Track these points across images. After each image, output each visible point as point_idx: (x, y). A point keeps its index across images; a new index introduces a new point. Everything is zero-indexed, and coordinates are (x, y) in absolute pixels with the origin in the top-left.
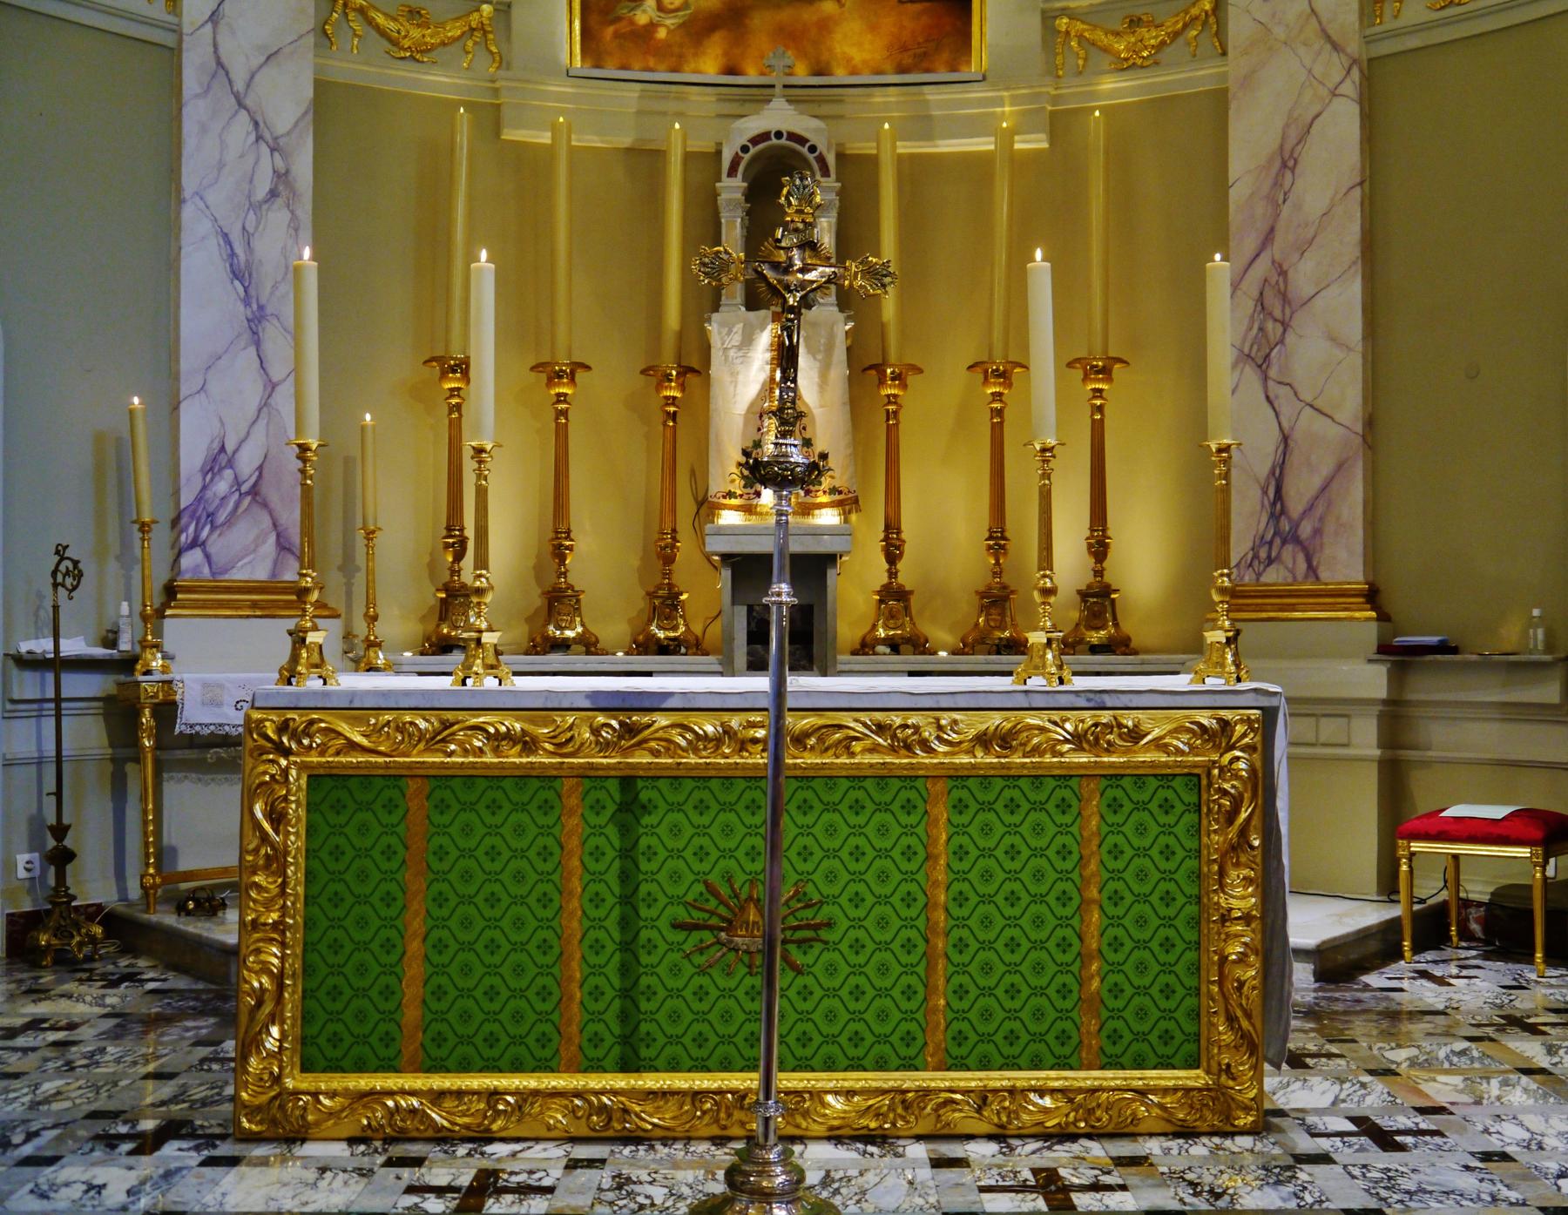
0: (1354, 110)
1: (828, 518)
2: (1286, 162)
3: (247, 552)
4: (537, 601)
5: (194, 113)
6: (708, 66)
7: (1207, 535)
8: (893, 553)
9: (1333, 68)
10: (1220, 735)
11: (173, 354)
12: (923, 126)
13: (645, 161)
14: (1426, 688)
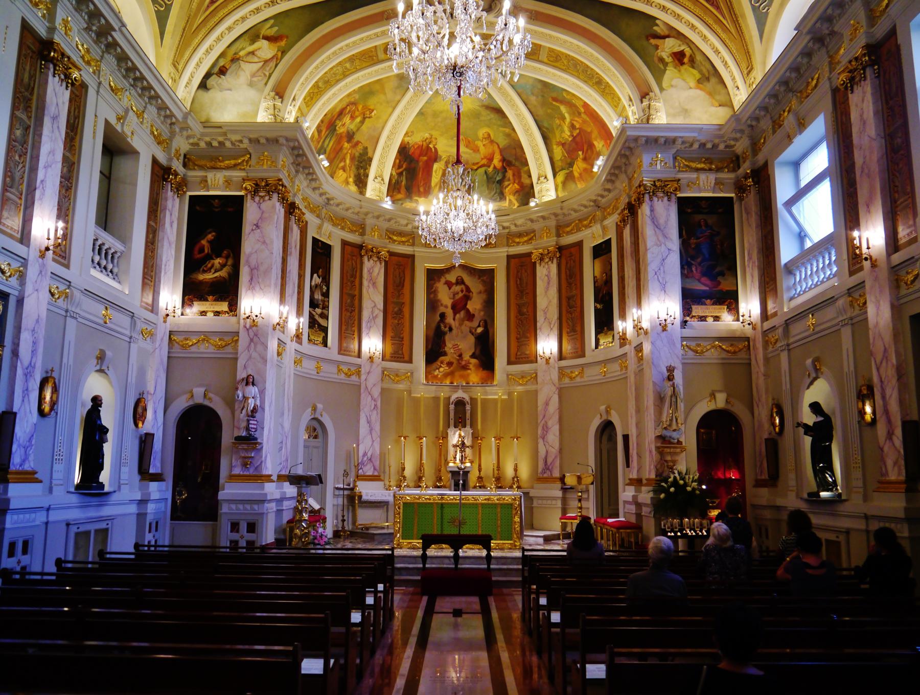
1: (468, 465)
2: (547, 404)
3: (369, 470)
4: (416, 478)
5: (363, 395)
6: (448, 382)
9: (554, 389)
10: (515, 499)
11: (358, 436)
12: (486, 393)
13: (436, 399)
14: (569, 495)
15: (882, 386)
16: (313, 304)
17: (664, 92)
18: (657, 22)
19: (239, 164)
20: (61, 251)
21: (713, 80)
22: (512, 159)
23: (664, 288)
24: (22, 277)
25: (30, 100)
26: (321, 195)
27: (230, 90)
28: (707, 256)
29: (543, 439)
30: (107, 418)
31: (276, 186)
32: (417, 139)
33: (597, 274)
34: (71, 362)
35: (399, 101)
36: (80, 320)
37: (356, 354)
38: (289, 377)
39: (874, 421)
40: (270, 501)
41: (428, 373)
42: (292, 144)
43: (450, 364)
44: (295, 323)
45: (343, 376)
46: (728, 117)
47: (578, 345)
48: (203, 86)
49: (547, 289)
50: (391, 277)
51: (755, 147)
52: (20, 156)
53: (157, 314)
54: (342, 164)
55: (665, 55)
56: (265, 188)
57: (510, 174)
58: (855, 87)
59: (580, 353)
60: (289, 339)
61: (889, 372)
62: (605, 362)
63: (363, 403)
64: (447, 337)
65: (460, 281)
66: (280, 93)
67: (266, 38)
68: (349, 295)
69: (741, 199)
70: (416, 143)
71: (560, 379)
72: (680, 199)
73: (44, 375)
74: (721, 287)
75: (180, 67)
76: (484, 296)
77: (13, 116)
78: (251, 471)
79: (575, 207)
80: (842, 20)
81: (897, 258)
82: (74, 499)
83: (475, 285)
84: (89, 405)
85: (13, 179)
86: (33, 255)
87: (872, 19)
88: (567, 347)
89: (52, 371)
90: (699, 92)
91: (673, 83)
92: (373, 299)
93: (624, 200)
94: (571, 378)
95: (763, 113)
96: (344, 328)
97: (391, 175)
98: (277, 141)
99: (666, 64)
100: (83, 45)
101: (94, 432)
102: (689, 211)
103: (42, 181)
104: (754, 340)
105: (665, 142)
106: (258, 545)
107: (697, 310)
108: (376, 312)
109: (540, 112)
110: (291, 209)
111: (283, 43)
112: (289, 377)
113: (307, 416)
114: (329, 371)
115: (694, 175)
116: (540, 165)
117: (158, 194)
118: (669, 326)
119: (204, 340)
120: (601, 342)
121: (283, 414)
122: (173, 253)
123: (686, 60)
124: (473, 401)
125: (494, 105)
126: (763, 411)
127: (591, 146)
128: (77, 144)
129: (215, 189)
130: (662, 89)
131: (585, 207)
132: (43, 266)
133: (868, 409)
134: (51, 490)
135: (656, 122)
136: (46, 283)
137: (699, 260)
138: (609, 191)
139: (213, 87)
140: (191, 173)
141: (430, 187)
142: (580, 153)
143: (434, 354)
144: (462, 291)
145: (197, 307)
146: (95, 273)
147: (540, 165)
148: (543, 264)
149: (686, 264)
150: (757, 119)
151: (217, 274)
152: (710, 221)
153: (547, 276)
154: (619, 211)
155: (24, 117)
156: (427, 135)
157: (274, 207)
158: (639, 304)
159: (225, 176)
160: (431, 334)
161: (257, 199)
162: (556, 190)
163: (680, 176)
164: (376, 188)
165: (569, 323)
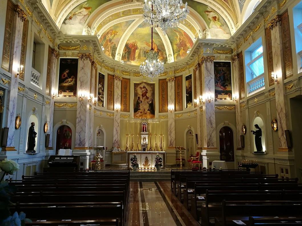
2: (171, 125)
6: (141, 118)
7: (167, 144)
8: (151, 145)
15: (280, 120)
16: (99, 94)
17: (210, 29)
18: (208, 7)
19: (77, 48)
20: (22, 75)
21: (225, 26)
22: (160, 49)
23: (210, 90)
24: (9, 83)
25: (11, 24)
26: (101, 59)
27: (73, 24)
28: (222, 79)
29: (170, 135)
30: (36, 130)
31: (89, 55)
32: (131, 42)
33: (187, 85)
34: (25, 111)
35: (126, 30)
36: (27, 98)
37: (113, 109)
38: (93, 116)
39: (277, 130)
40: (88, 155)
41: (134, 115)
42: (94, 43)
43: (141, 112)
44: (95, 99)
45: (108, 116)
46: (230, 38)
47: (181, 107)
48: (64, 23)
50: (123, 86)
51: (238, 47)
52: (8, 43)
53: (51, 96)
54: (108, 49)
55: (210, 18)
56: (85, 56)
57: (160, 54)
58: (273, 28)
59: (181, 109)
60: (92, 104)
61: (283, 116)
62: (190, 112)
63: (115, 124)
64: (140, 104)
65: (144, 87)
66: (89, 26)
67: (85, 8)
68: (110, 91)
69: (233, 63)
70: (131, 43)
71: (175, 117)
72: (215, 62)
73: (17, 116)
74: (226, 89)
75: (57, 16)
76: (152, 92)
77: (5, 30)
78: (81, 146)
79: (181, 64)
80: (270, 7)
81: (286, 81)
82: (27, 156)
83: (149, 88)
84: (31, 125)
85: (6, 51)
86: (13, 77)
87: (279, 7)
88: (177, 108)
89: (19, 114)
90: (220, 29)
91: (213, 26)
92: (118, 92)
93: (196, 63)
94: (178, 117)
95: (241, 36)
96: (109, 101)
97: (123, 53)
98: (89, 41)
99: (210, 20)
100: (27, 7)
101: (32, 134)
102: (217, 66)
103: (15, 52)
104: (237, 106)
105: (211, 44)
106: (84, 169)
107: (219, 96)
108: (119, 96)
109: (170, 34)
110: (93, 63)
111: (90, 10)
112: (93, 116)
113: (98, 128)
114: (104, 115)
115: (219, 55)
116: (169, 51)
117: (50, 57)
118: (211, 101)
119: (65, 104)
120: (188, 106)
121: (91, 128)
122: (55, 76)
123: (217, 19)
124: (148, 124)
125: (156, 32)
126: (239, 127)
127: (186, 45)
128: (26, 40)
129: (69, 56)
130: (209, 28)
131: (184, 64)
132: (16, 80)
133: (275, 126)
134: (19, 153)
135: (208, 38)
136: (17, 86)
137: (220, 81)
138: (191, 59)
139: (67, 23)
140: (60, 51)
141: (135, 57)
142: (182, 47)
143: (136, 110)
144: (145, 90)
145: (63, 94)
146: (32, 83)
147: (169, 51)
148: (170, 82)
149: (216, 82)
150: (239, 38)
151: (70, 84)
152: (223, 70)
153: (171, 87)
154: (195, 66)
155: (9, 30)
156: (134, 41)
157: (88, 62)
158: (201, 94)
159: (72, 52)
160: (136, 103)
161: (83, 60)
162: (174, 59)
163: (214, 55)
164: (118, 58)
165: (178, 100)
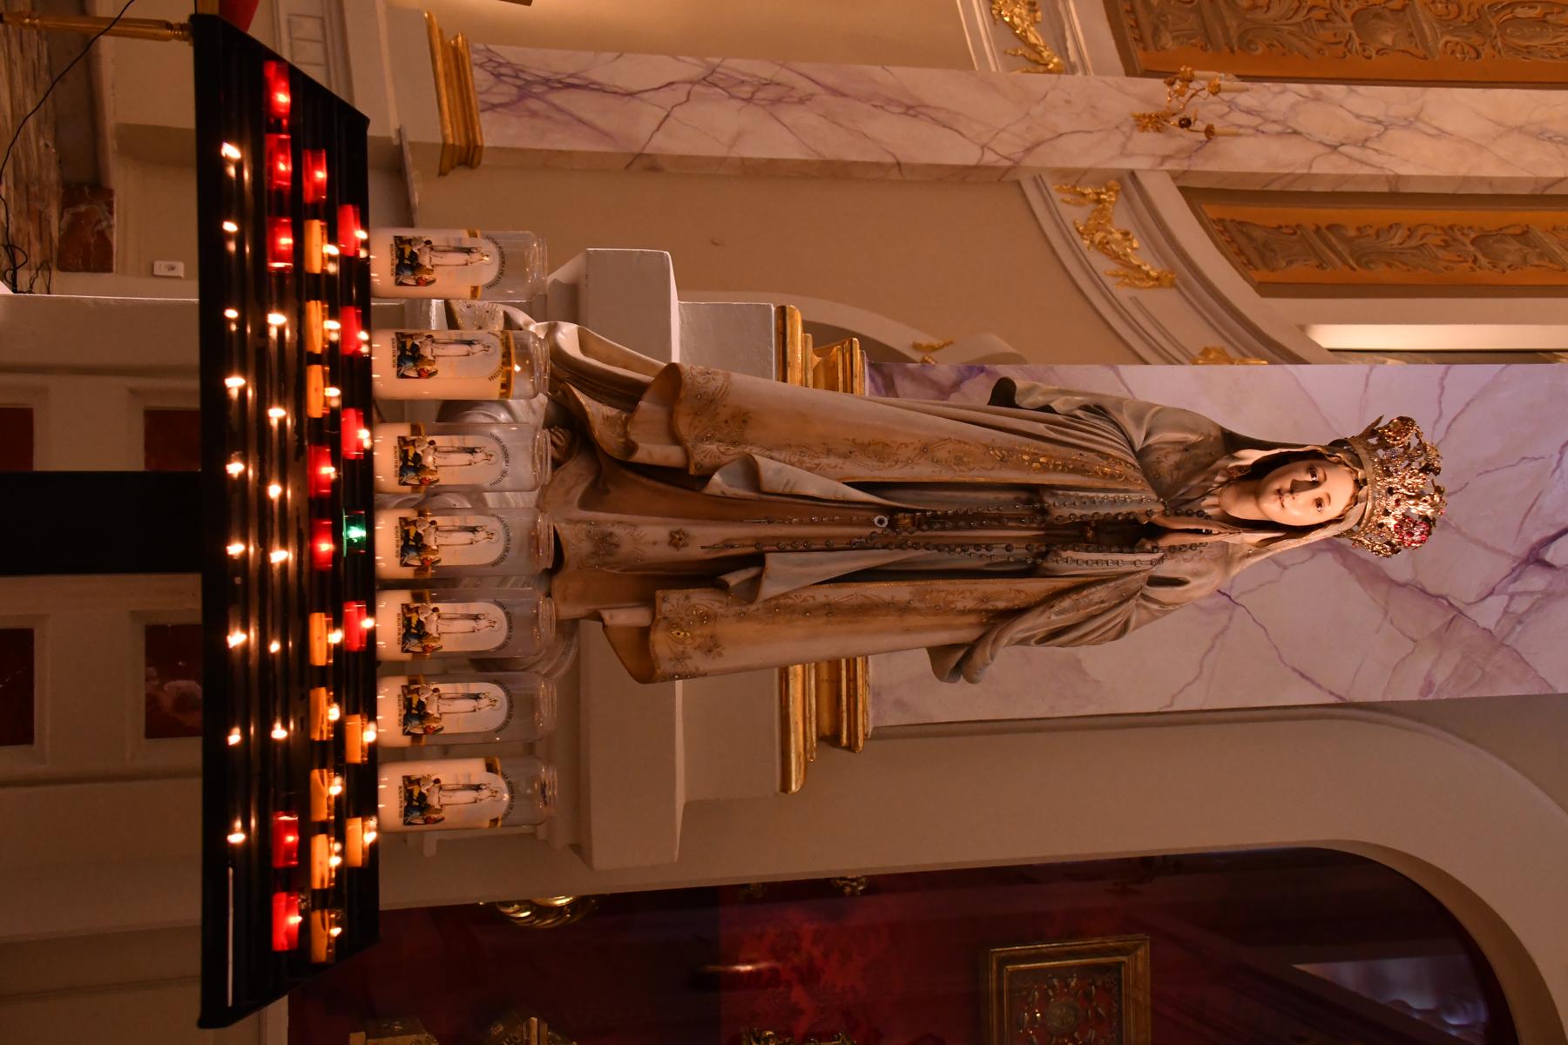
0: (972, 161)
2: (912, 109)
49: (1541, 135)
71: (1072, 178)
